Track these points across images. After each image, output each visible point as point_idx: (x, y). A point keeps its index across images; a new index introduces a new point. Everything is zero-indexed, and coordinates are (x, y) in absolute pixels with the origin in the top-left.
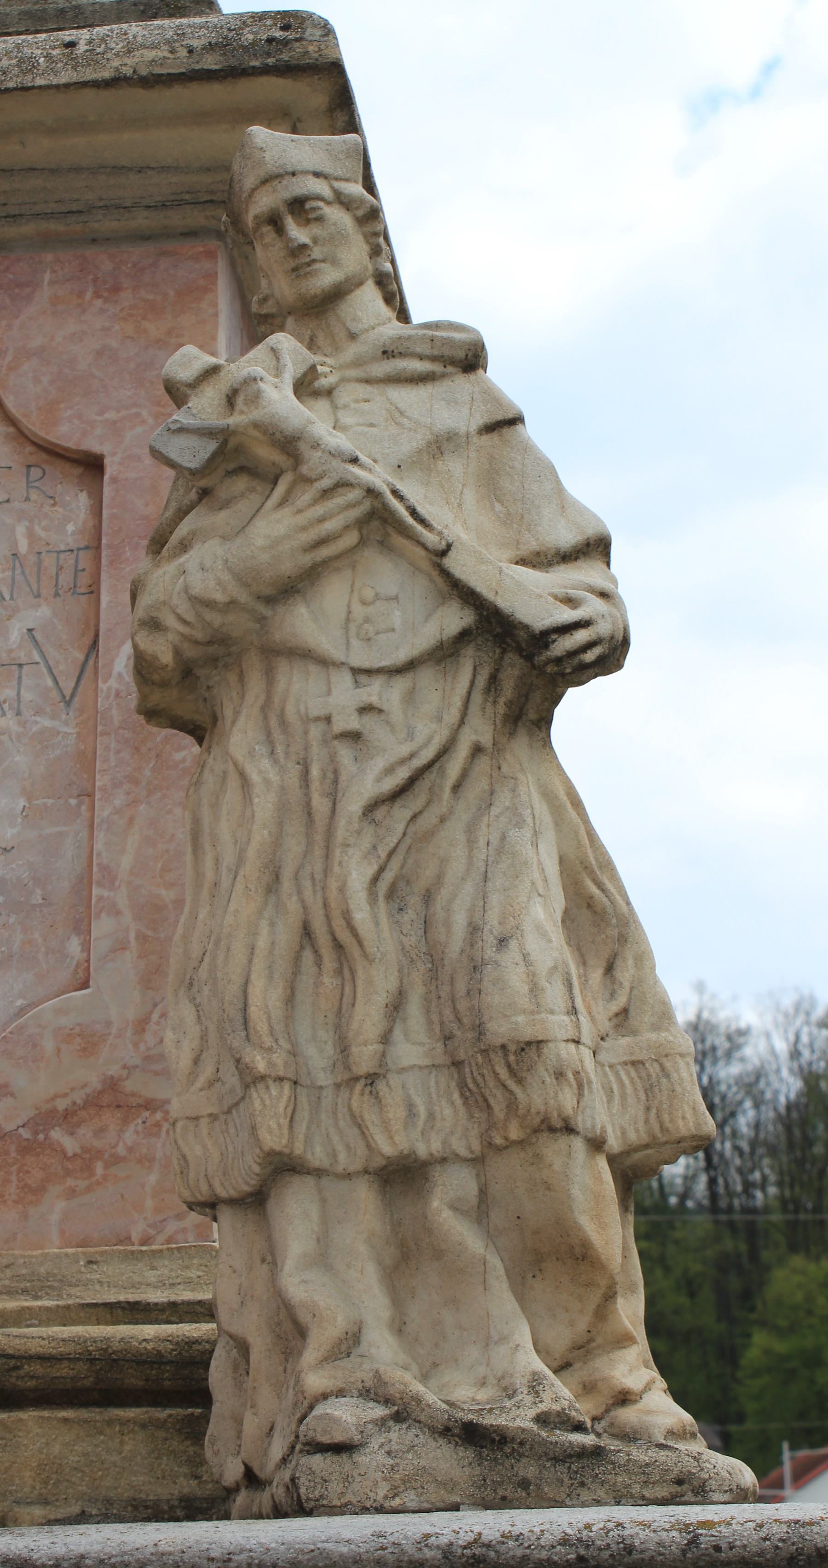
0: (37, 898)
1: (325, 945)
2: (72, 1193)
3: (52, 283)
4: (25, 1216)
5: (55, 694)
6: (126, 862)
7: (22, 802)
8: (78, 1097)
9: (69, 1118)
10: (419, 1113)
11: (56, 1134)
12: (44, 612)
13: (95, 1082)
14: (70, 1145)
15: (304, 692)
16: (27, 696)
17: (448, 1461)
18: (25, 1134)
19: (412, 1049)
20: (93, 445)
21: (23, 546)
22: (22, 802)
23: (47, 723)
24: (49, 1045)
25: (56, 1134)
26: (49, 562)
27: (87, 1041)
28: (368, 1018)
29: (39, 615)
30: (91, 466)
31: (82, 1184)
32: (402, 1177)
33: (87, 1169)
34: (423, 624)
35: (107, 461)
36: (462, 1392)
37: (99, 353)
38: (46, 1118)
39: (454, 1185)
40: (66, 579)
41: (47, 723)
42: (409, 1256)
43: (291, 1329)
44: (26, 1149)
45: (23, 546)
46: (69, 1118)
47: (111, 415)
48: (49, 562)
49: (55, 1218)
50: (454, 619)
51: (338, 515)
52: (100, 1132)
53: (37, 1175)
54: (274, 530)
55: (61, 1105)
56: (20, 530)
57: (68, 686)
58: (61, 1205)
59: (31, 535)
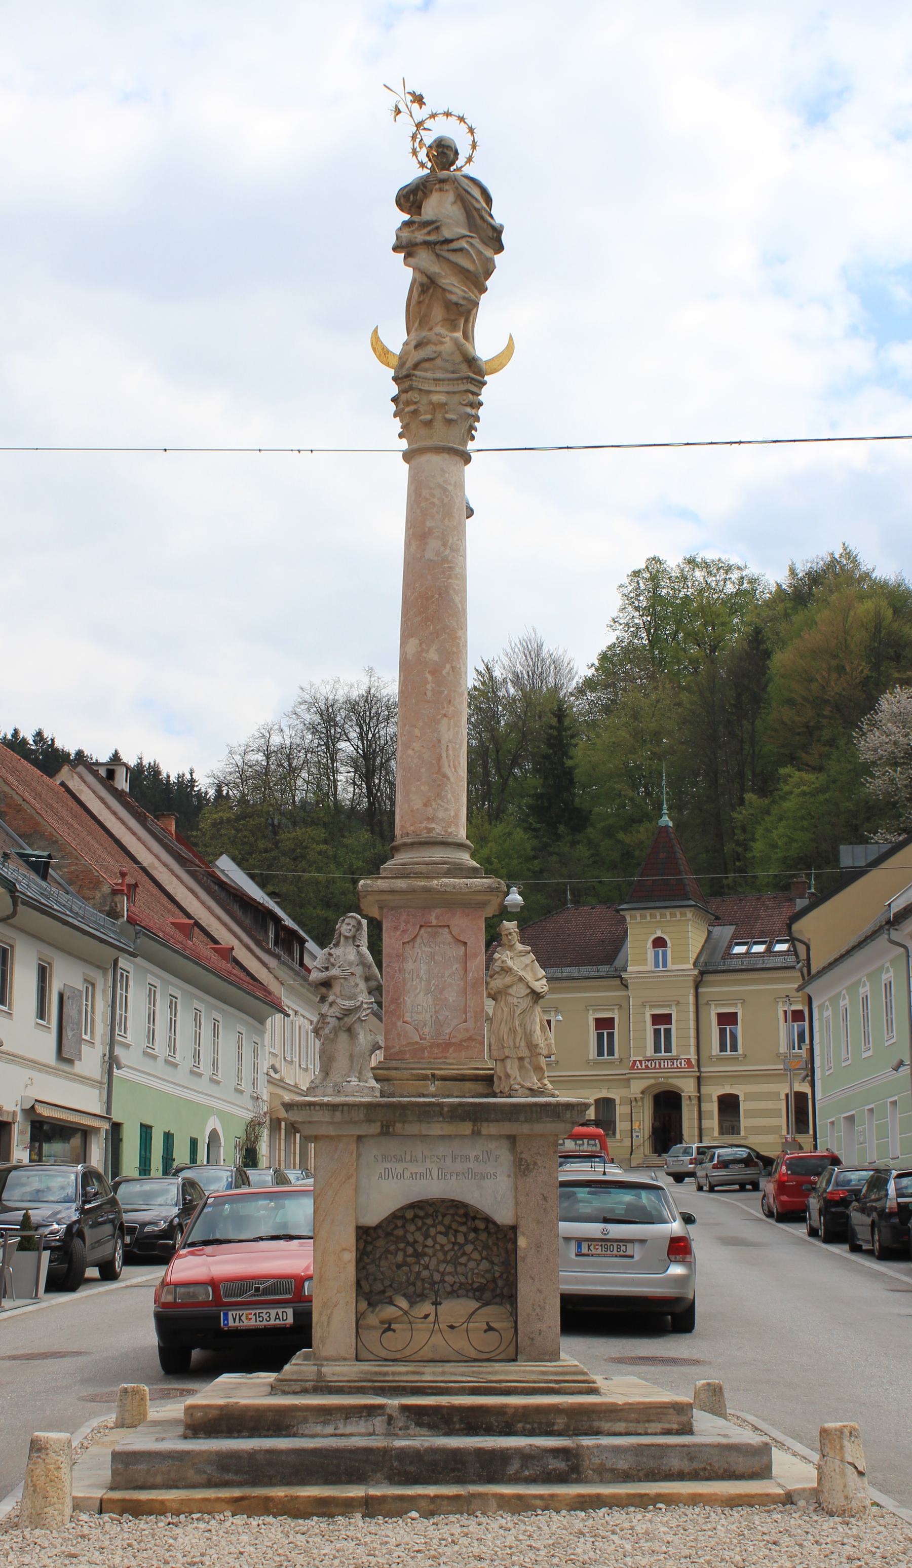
1: (513, 1031)
9: (465, 1041)
10: (524, 1052)
15: (510, 999)
17: (527, 1092)
19: (523, 1044)
27: (467, 1030)
28: (518, 1040)
30: (466, 943)
32: (521, 1059)
34: (524, 991)
36: (528, 1085)
38: (462, 1041)
39: (527, 1060)
42: (521, 1068)
43: (508, 1076)
46: (465, 1041)
50: (529, 991)
51: (516, 979)
54: (508, 980)
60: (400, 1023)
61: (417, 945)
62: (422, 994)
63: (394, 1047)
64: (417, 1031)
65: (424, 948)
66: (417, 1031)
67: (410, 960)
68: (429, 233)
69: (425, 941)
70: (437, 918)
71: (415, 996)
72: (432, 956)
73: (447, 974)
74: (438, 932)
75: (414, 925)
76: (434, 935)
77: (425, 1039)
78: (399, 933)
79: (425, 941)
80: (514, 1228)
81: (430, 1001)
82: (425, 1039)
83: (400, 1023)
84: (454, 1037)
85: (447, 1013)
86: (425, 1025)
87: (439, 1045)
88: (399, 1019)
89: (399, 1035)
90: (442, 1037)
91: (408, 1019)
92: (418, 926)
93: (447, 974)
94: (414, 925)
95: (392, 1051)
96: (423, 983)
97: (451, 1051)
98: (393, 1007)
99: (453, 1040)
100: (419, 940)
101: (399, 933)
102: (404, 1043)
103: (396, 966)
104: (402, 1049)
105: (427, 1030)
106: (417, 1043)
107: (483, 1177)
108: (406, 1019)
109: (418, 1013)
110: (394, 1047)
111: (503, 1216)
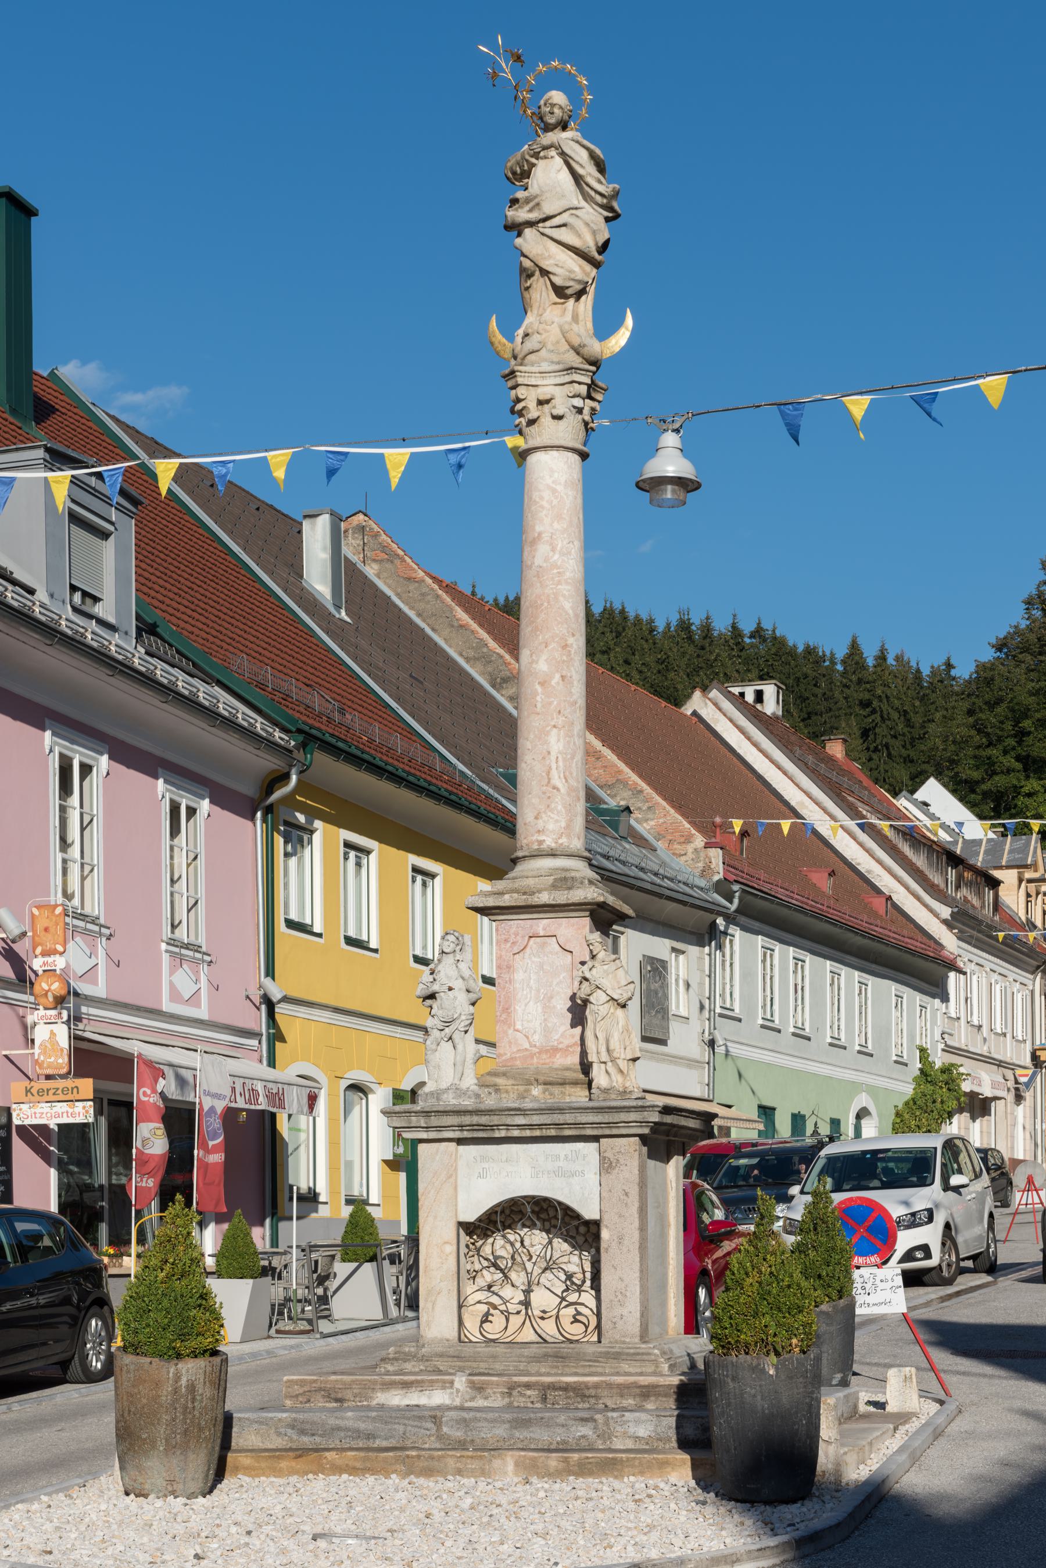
29: (564, 974)
38: (568, 1046)
60: (510, 1031)
64: (527, 1037)
66: (527, 1037)
68: (531, 211)
70: (544, 929)
72: (541, 966)
73: (555, 983)
74: (545, 943)
75: (523, 937)
78: (509, 945)
80: (597, 1224)
81: (540, 1009)
83: (510, 1031)
85: (555, 1021)
87: (547, 1051)
89: (510, 1042)
91: (519, 1026)
92: (527, 938)
93: (555, 983)
94: (523, 937)
97: (558, 1056)
98: (504, 1016)
99: (560, 1046)
100: (528, 950)
101: (509, 945)
105: (536, 1037)
106: (526, 1050)
107: (573, 1174)
111: (589, 1212)
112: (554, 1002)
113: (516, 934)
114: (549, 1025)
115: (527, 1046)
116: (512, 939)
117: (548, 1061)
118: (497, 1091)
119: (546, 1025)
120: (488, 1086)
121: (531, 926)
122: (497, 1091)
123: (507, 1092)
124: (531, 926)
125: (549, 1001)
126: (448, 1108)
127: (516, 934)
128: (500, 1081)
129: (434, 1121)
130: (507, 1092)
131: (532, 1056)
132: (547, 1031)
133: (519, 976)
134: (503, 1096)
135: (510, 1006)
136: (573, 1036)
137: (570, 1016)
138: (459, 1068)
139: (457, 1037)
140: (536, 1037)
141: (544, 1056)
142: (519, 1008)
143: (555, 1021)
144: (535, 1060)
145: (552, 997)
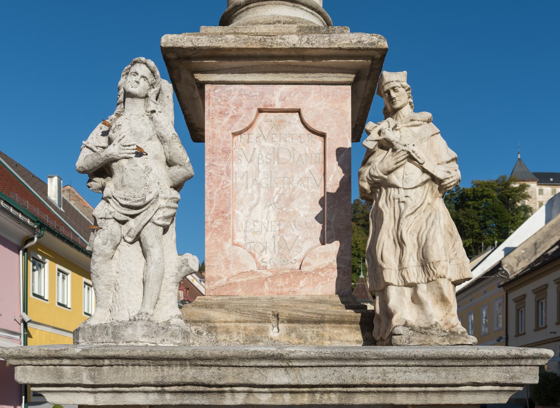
0: (313, 226)
2: (323, 284)
3: (314, 93)
4: (314, 288)
5: (315, 184)
6: (333, 220)
7: (309, 207)
8: (324, 266)
11: (320, 273)
12: (313, 166)
13: (327, 264)
14: (323, 275)
16: (310, 184)
18: (314, 272)
20: (324, 131)
21: (308, 152)
22: (309, 207)
23: (314, 190)
24: (318, 255)
25: (320, 273)
26: (313, 156)
30: (323, 135)
31: (325, 283)
33: (326, 280)
35: (327, 135)
37: (325, 110)
38: (317, 270)
40: (317, 160)
41: (314, 190)
44: (314, 275)
45: (308, 152)
46: (322, 270)
47: (328, 124)
48: (313, 156)
49: (320, 289)
52: (328, 273)
53: (316, 280)
55: (321, 267)
56: (307, 148)
57: (318, 183)
58: (321, 286)
59: (309, 149)
60: (228, 245)
61: (253, 137)
62: (260, 207)
63: (220, 278)
64: (254, 256)
65: (263, 143)
66: (254, 256)
67: (244, 160)
69: (266, 133)
70: (282, 99)
71: (251, 209)
73: (296, 179)
74: (281, 121)
75: (249, 109)
76: (279, 125)
77: (265, 268)
79: (266, 133)
82: (265, 268)
83: (228, 245)
84: (307, 264)
85: (297, 233)
86: (265, 249)
87: (285, 276)
88: (226, 240)
89: (227, 262)
90: (290, 266)
91: (239, 239)
92: (255, 111)
93: (296, 179)
94: (249, 109)
95: (217, 283)
96: (262, 191)
97: (302, 283)
98: (218, 222)
100: (255, 130)
101: (226, 119)
102: (235, 273)
103: (223, 166)
104: (232, 280)
105: (267, 256)
106: (253, 272)
108: (236, 241)
109: (255, 233)
110: (220, 278)
112: (295, 205)
113: (239, 105)
114: (287, 239)
115: (253, 266)
116: (232, 111)
117: (286, 290)
118: (212, 330)
119: (282, 239)
120: (195, 322)
121: (262, 94)
122: (212, 330)
123: (228, 331)
124: (262, 94)
125: (287, 205)
126: (138, 352)
127: (239, 105)
128: (216, 315)
129: (108, 375)
130: (228, 331)
131: (261, 282)
132: (283, 247)
133: (241, 167)
134: (221, 337)
135: (228, 209)
136: (326, 255)
137: (319, 226)
138: (152, 287)
139: (151, 234)
140: (267, 256)
141: (280, 283)
142: (240, 214)
143: (297, 233)
144: (266, 288)
145: (291, 199)
